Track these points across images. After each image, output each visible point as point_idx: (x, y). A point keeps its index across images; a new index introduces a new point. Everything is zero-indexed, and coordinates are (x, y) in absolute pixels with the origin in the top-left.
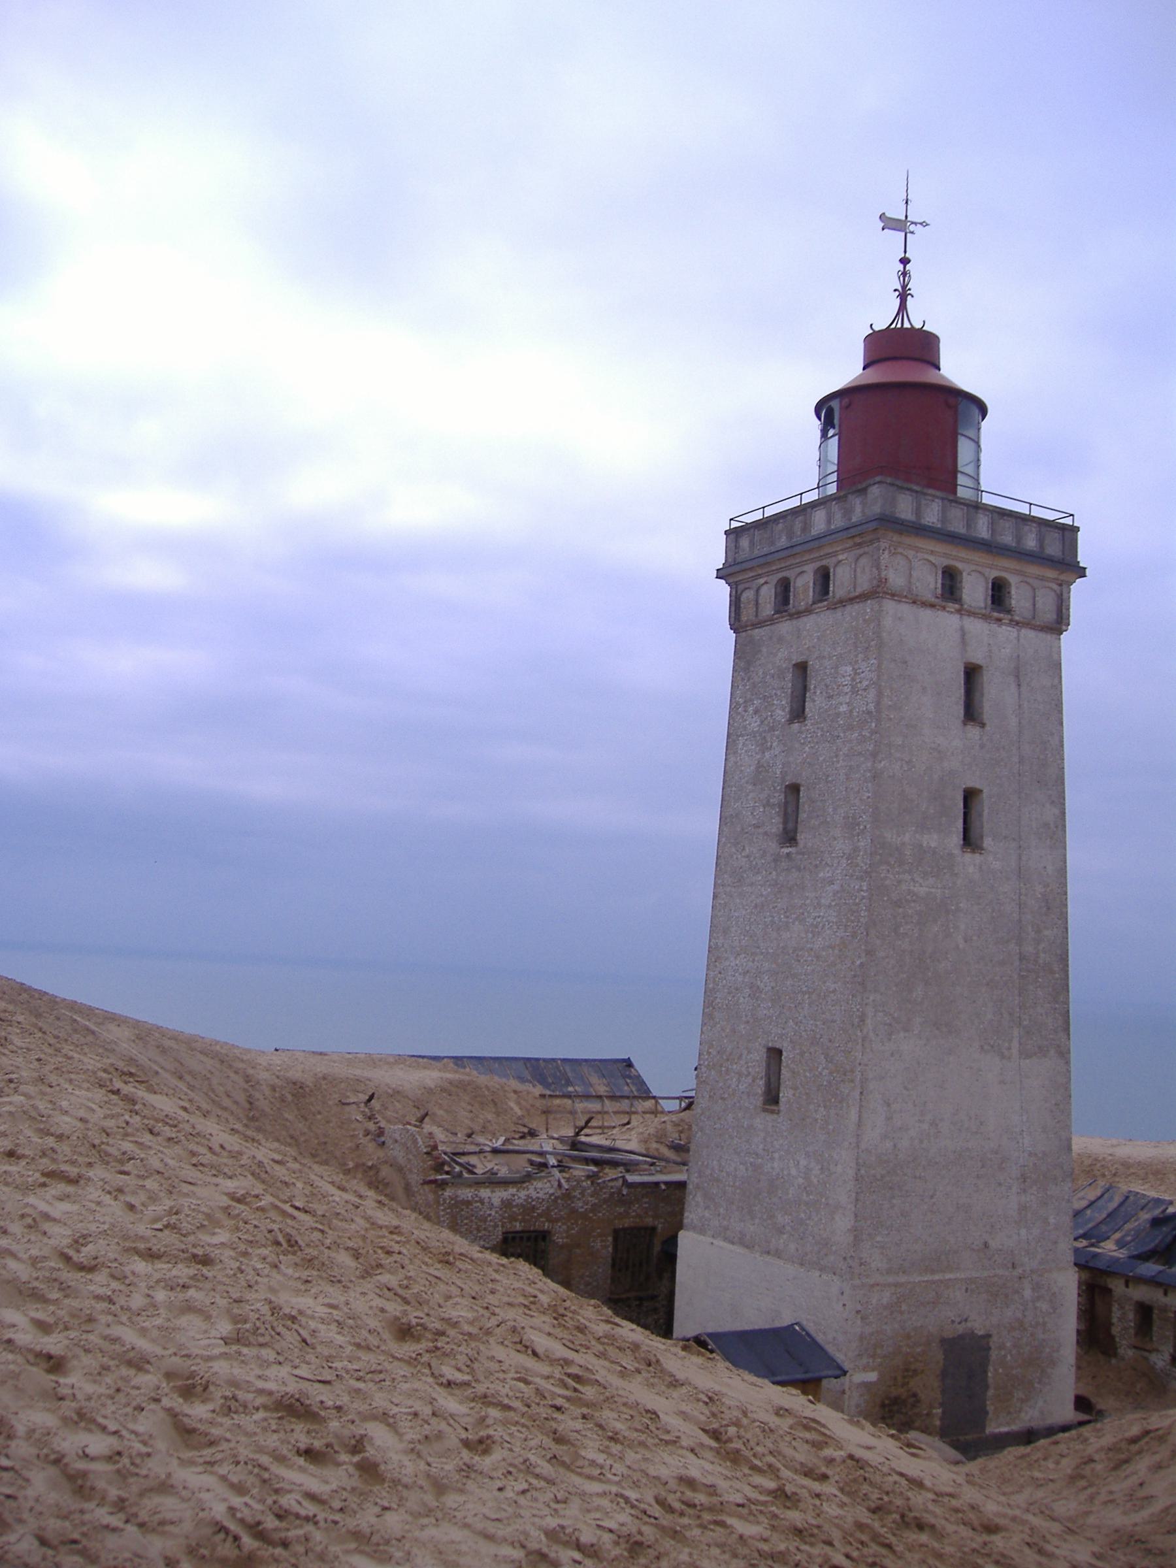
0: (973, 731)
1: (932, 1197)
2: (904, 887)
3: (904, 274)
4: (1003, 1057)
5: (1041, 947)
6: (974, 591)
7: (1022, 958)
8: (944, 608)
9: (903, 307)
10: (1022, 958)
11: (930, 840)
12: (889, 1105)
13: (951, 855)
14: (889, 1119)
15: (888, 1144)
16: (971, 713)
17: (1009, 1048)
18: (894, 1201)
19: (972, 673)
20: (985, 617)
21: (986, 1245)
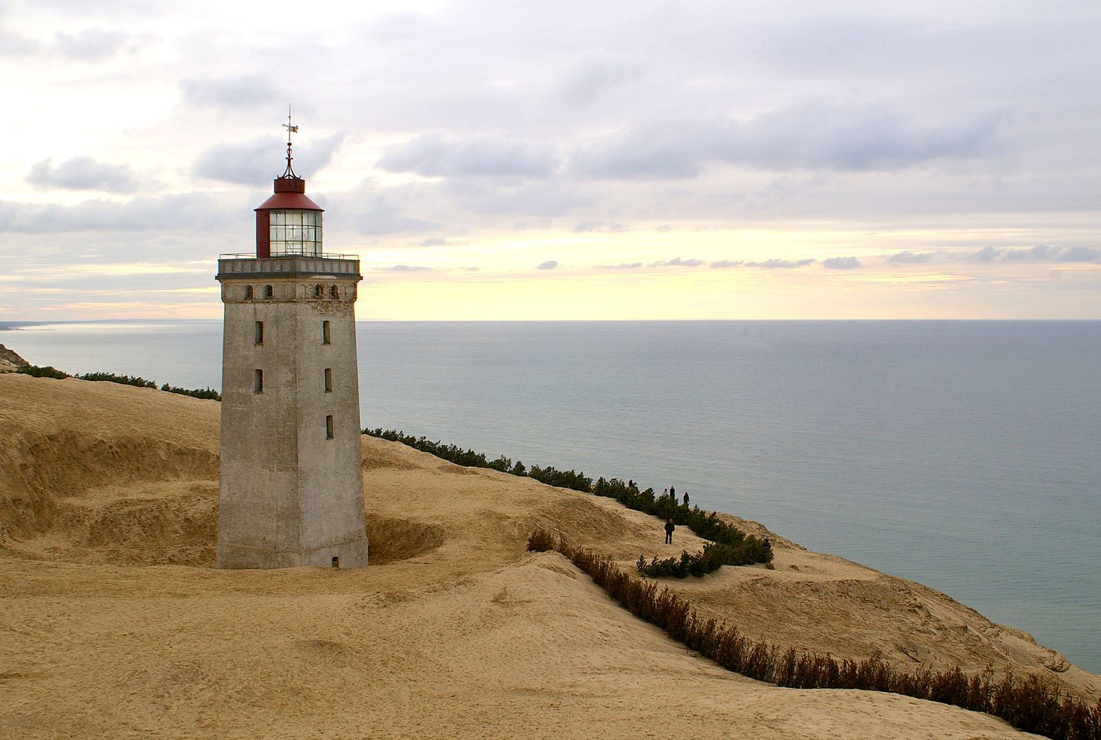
0: (259, 348)
2: (233, 408)
3: (289, 150)
4: (270, 470)
5: (286, 429)
6: (259, 292)
7: (279, 433)
8: (247, 302)
9: (289, 165)
10: (279, 433)
11: (243, 391)
12: (229, 485)
13: (250, 395)
15: (229, 498)
16: (260, 340)
17: (273, 467)
19: (260, 325)
20: (263, 302)
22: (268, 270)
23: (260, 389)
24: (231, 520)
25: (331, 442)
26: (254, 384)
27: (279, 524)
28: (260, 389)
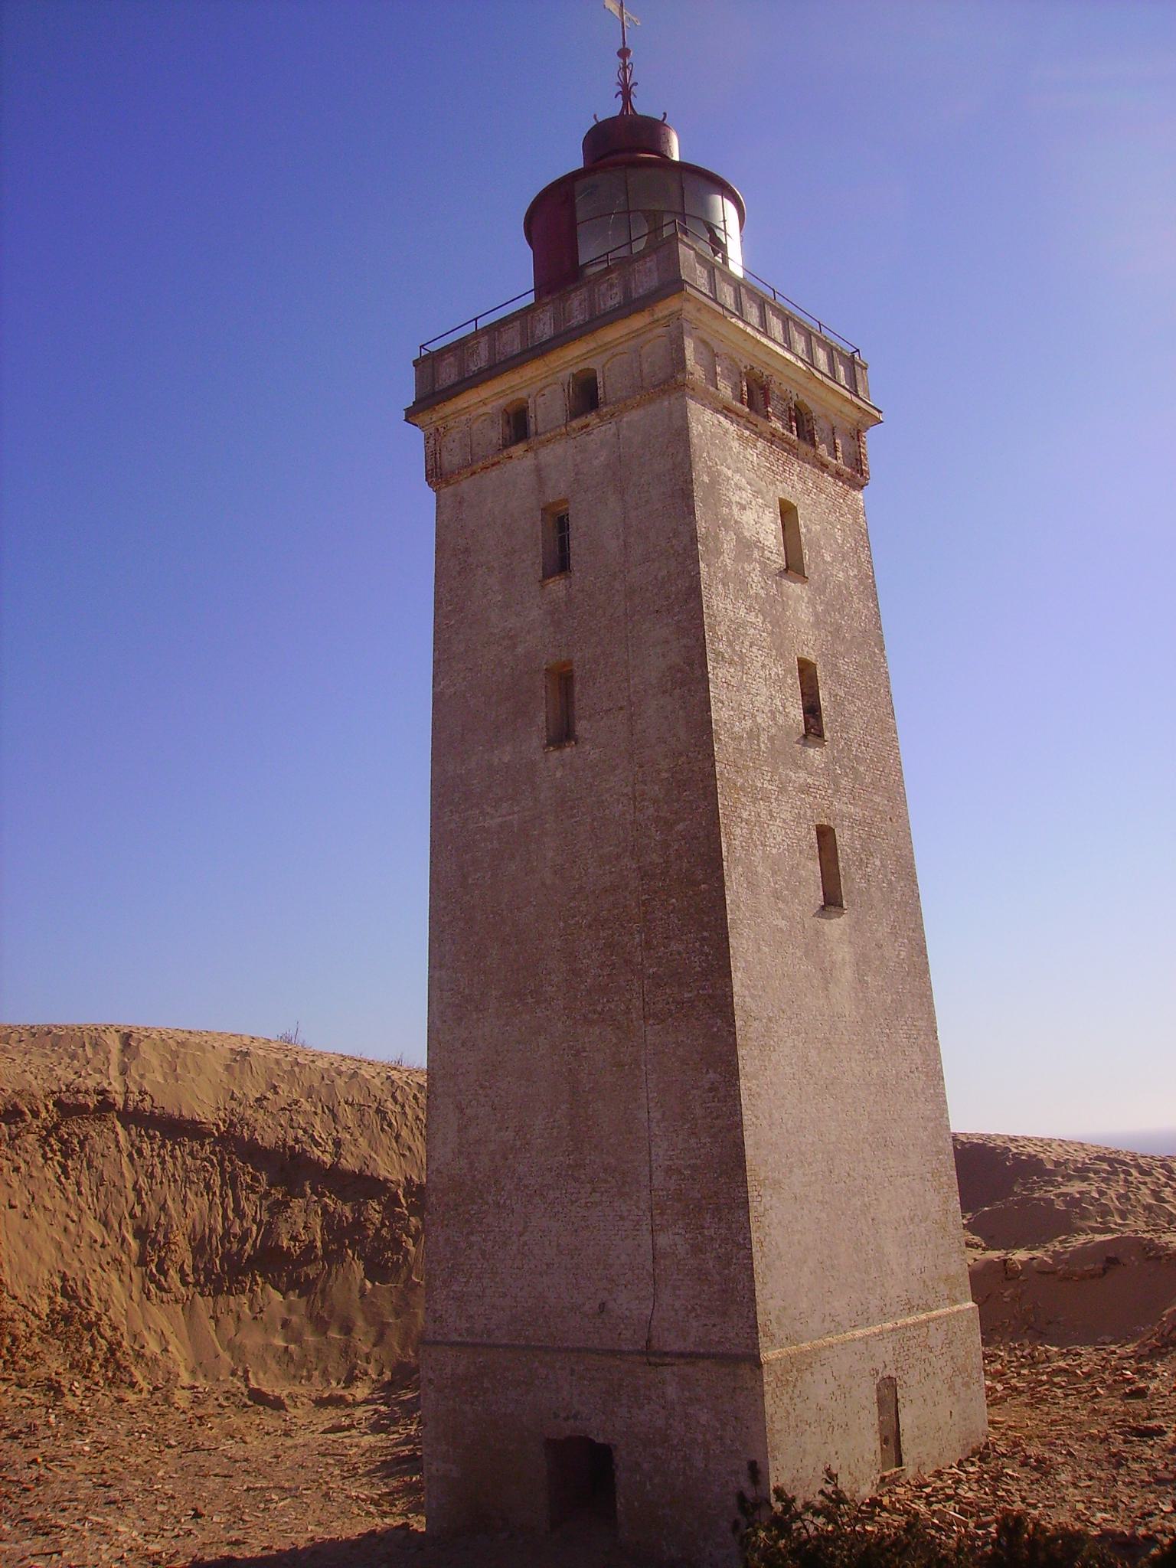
0: (557, 586)
1: (521, 1235)
3: (625, 67)
12: (462, 1111)
14: (462, 1129)
17: (628, 1011)
18: (473, 1238)
21: (602, 1307)
22: (578, 318)
23: (563, 734)
24: (471, 1246)
25: (836, 926)
26: (541, 718)
27: (663, 1240)
28: (563, 734)
